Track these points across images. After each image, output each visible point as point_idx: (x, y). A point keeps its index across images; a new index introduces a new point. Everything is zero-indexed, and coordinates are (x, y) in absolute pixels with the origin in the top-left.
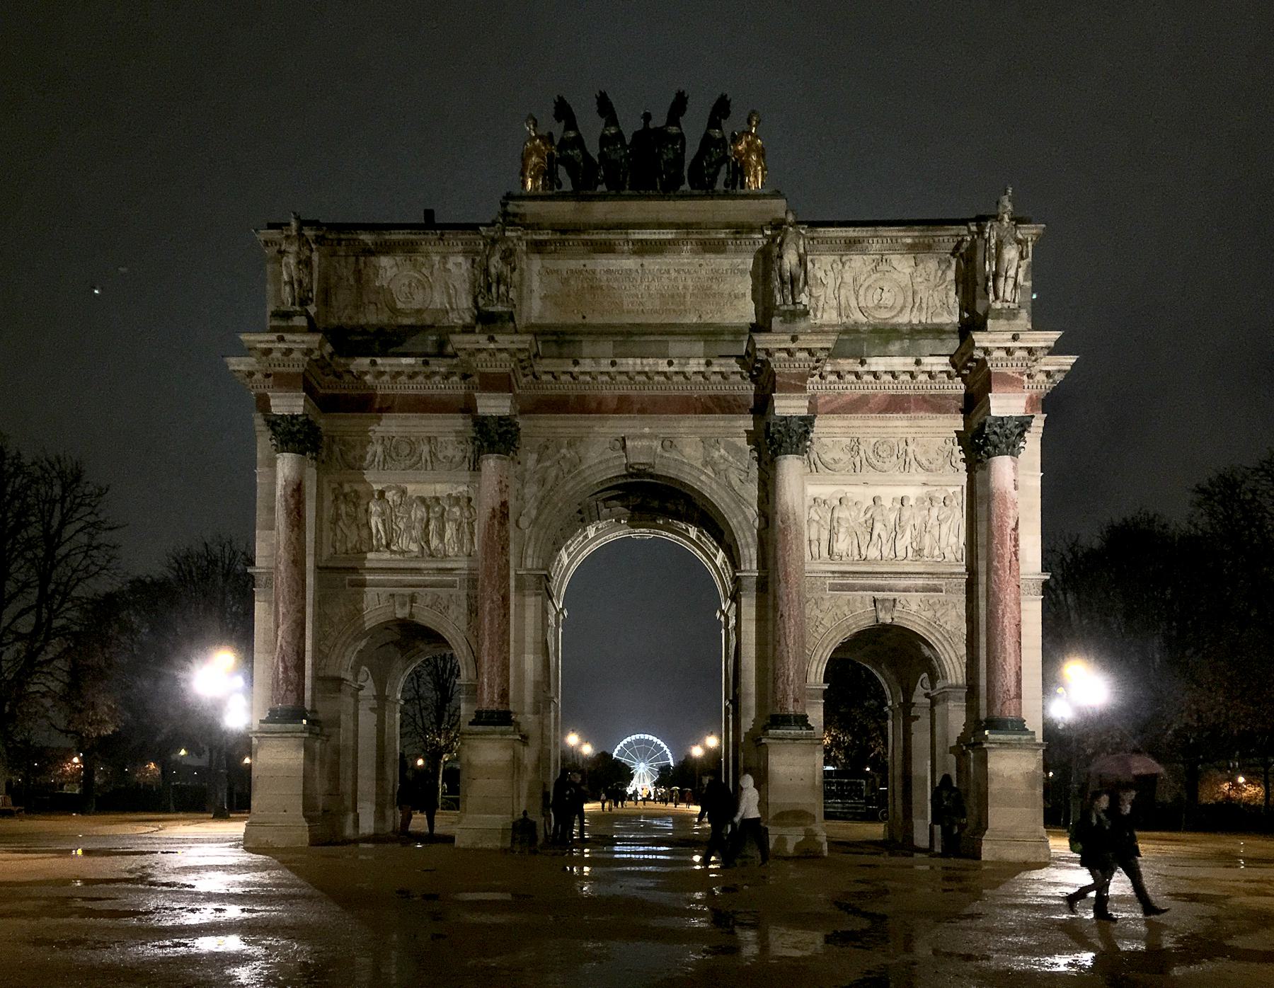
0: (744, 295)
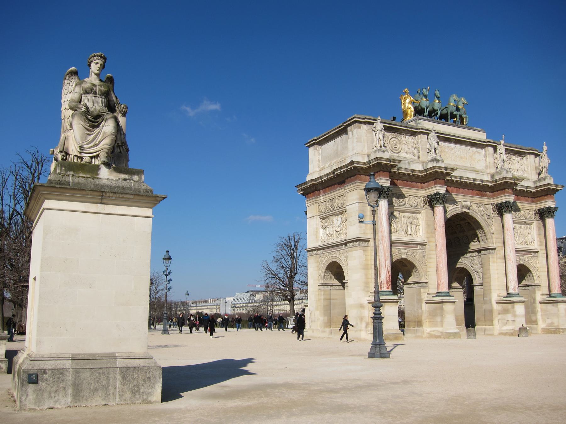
0: (480, 160)
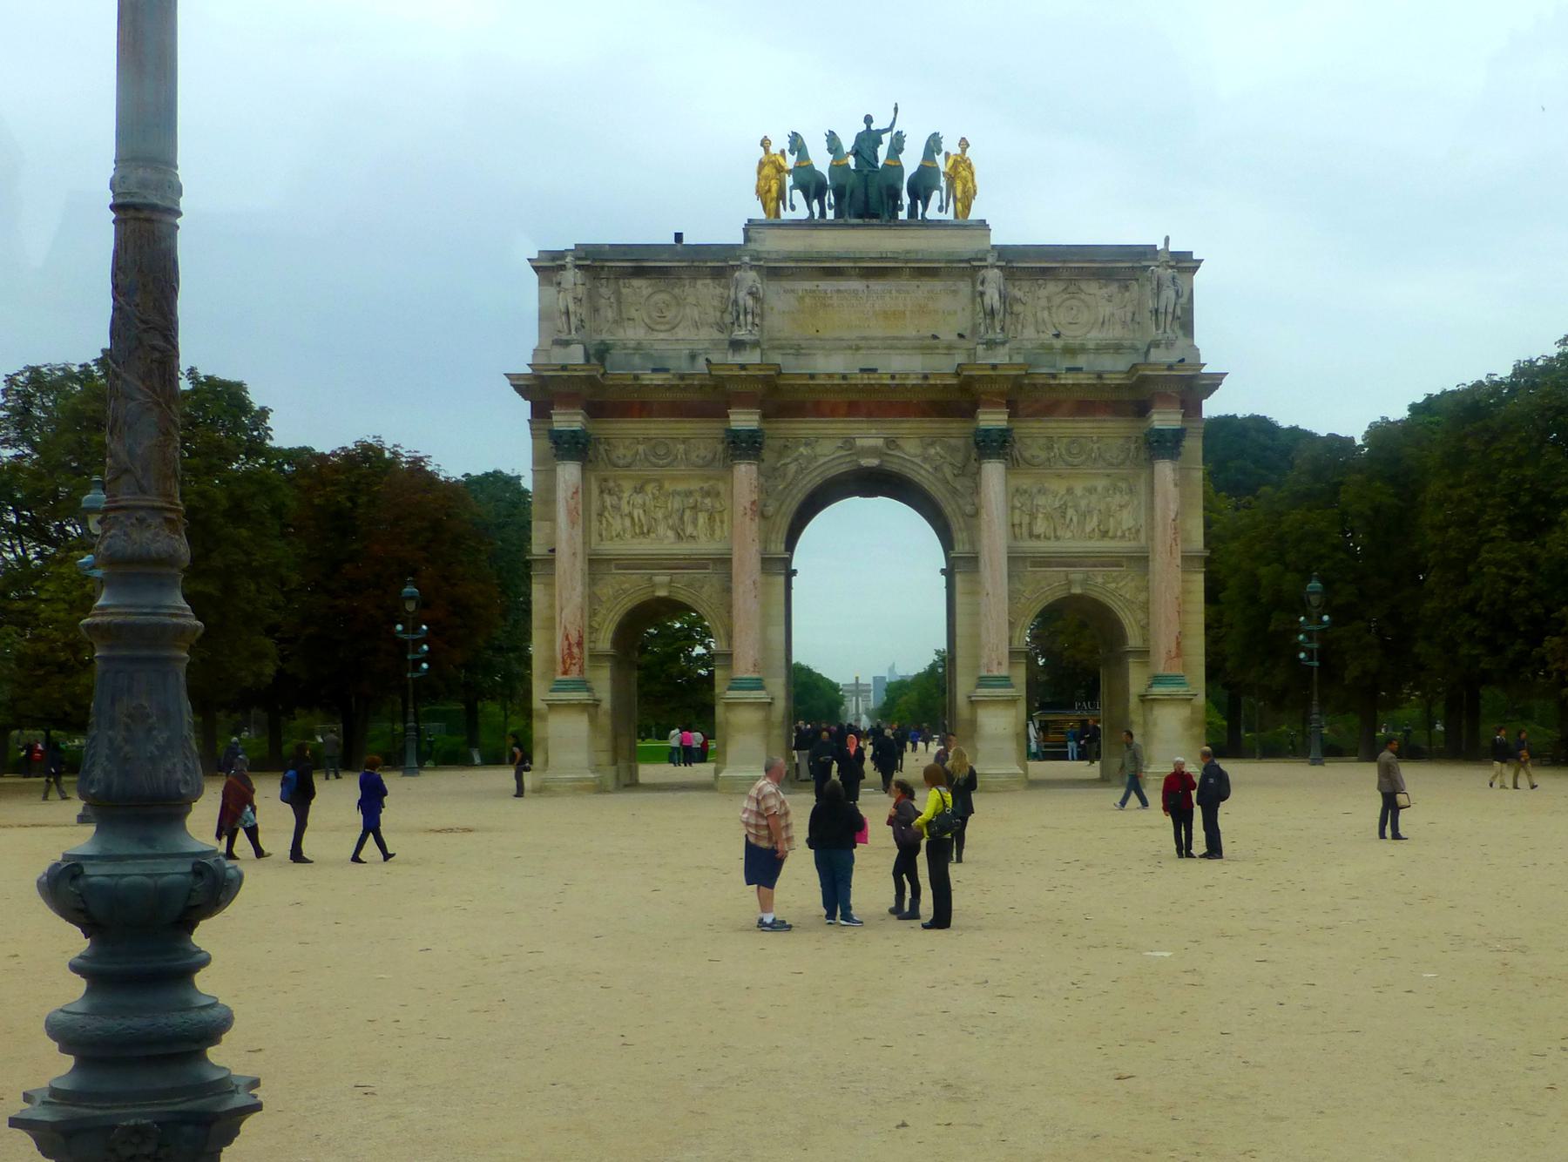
0: (955, 312)
